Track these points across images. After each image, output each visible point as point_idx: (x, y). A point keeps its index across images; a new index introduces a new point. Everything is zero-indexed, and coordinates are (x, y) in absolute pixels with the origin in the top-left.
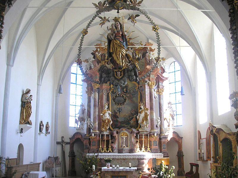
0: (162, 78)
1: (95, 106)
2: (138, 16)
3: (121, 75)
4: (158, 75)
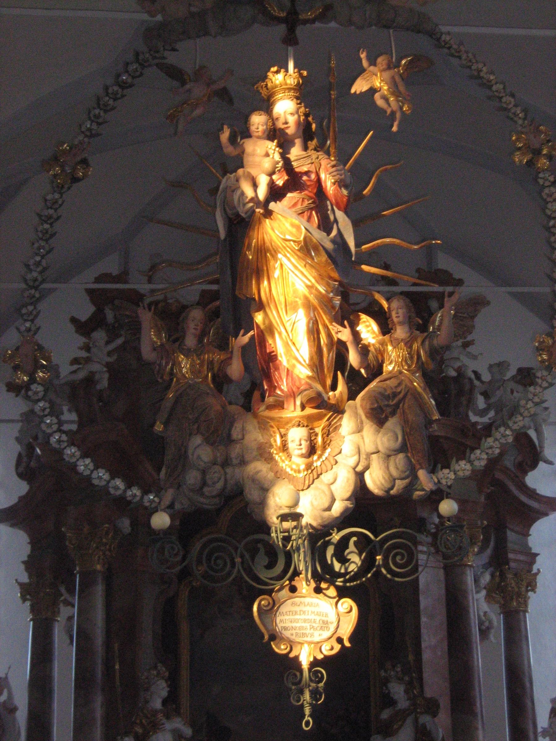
0: (523, 498)
1: (83, 683)
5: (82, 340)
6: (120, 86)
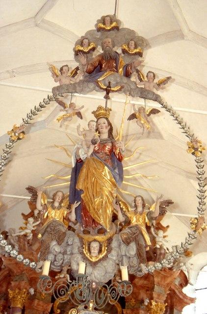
2: (154, 111)
3: (100, 251)
4: (171, 290)
5: (24, 221)
6: (41, 107)
